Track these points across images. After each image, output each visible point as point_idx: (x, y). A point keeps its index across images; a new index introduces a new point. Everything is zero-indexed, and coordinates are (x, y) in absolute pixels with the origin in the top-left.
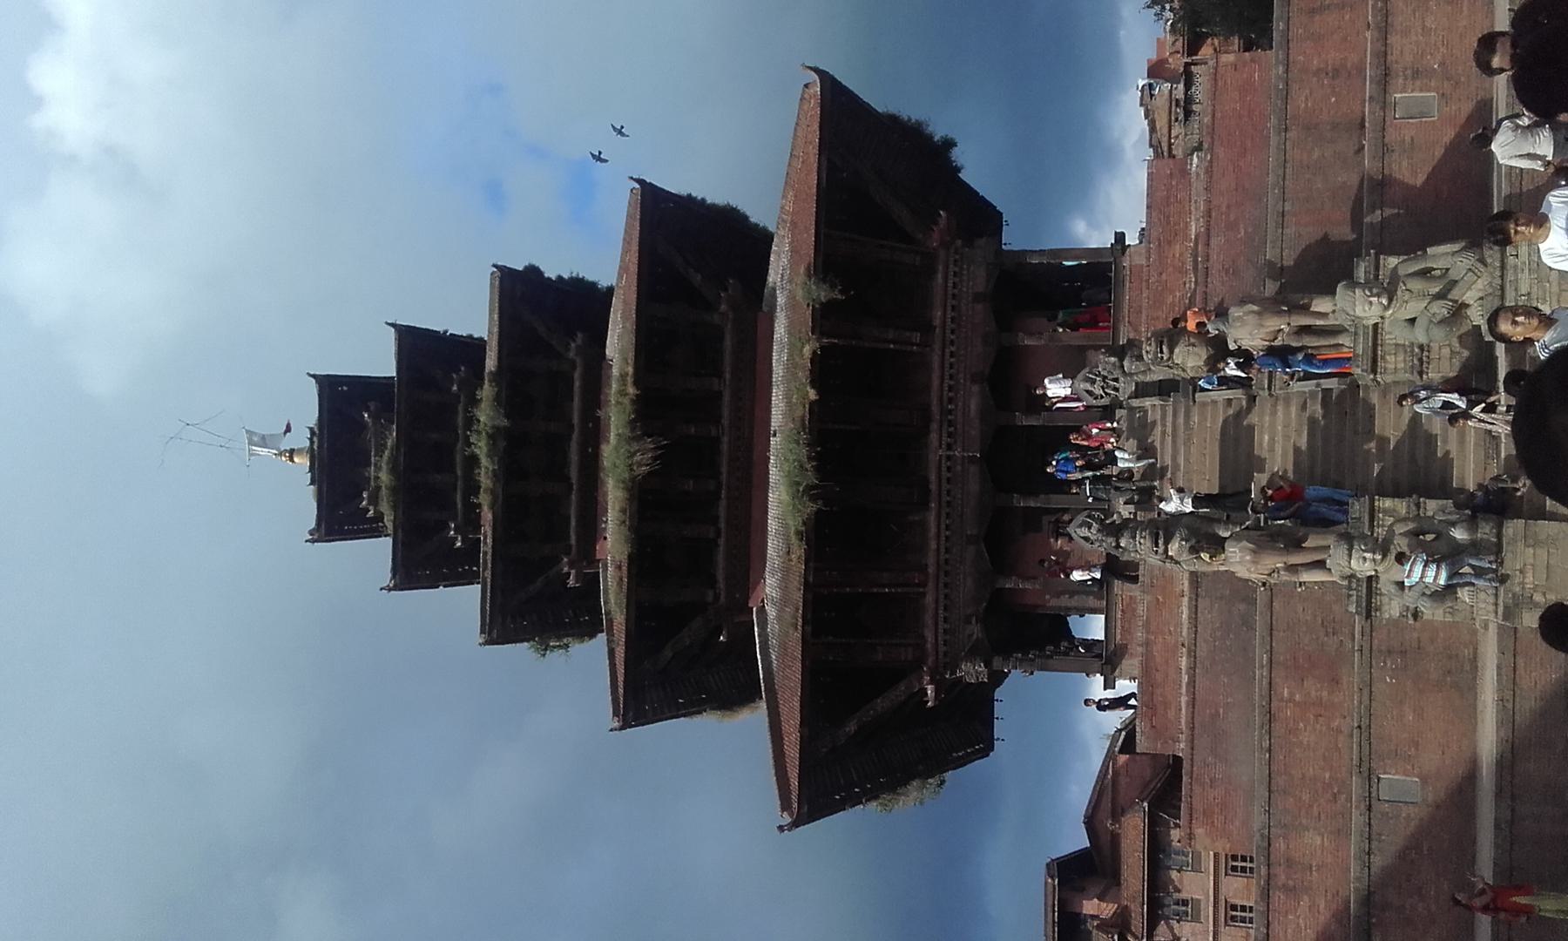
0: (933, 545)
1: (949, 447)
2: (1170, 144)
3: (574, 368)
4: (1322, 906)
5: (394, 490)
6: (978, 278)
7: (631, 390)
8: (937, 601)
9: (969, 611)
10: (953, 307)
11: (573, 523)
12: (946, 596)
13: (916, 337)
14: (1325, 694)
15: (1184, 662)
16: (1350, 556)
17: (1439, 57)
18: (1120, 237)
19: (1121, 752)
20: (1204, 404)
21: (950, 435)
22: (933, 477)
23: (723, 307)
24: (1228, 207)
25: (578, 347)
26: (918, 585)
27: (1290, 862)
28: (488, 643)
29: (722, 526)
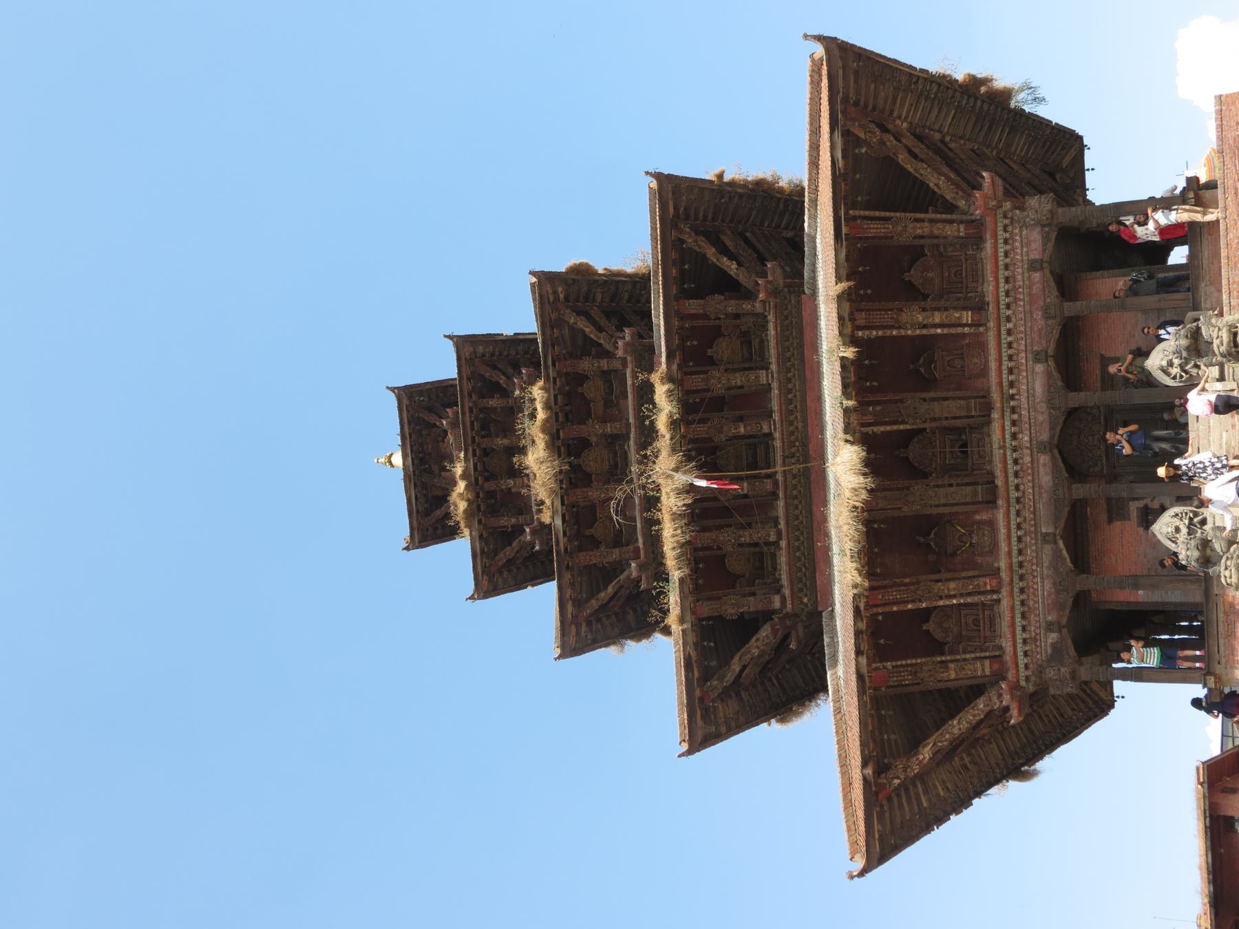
3: (625, 365)
8: (1013, 609)
10: (1007, 280)
12: (1023, 603)
13: (967, 317)
21: (1014, 423)
22: (998, 472)
23: (762, 296)
25: (626, 344)
26: (993, 592)
29: (782, 525)
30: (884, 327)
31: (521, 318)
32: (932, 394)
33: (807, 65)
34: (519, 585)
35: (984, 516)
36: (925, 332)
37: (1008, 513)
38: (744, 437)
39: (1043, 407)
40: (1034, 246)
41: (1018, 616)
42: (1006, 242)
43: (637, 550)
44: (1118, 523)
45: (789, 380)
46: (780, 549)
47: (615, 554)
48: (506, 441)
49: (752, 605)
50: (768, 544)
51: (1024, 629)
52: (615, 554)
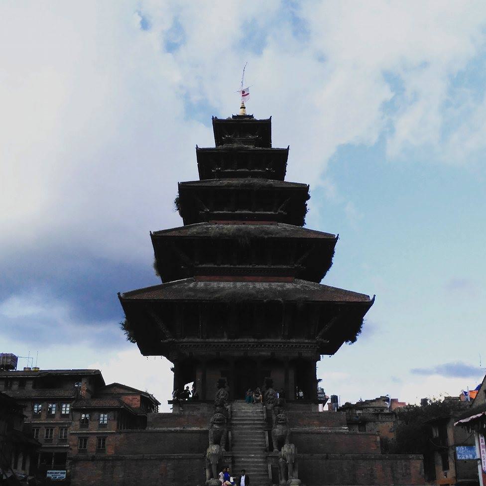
0: (215, 341)
2: (367, 408)
4: (99, 478)
5: (231, 149)
6: (307, 354)
7: (266, 237)
8: (197, 342)
9: (193, 353)
11: (221, 212)
14: (169, 477)
15: (178, 428)
19: (141, 396)
20: (264, 434)
21: (253, 345)
22: (239, 340)
28: (179, 184)
34: (198, 161)
35: (225, 334)
37: (225, 342)
46: (214, 265)
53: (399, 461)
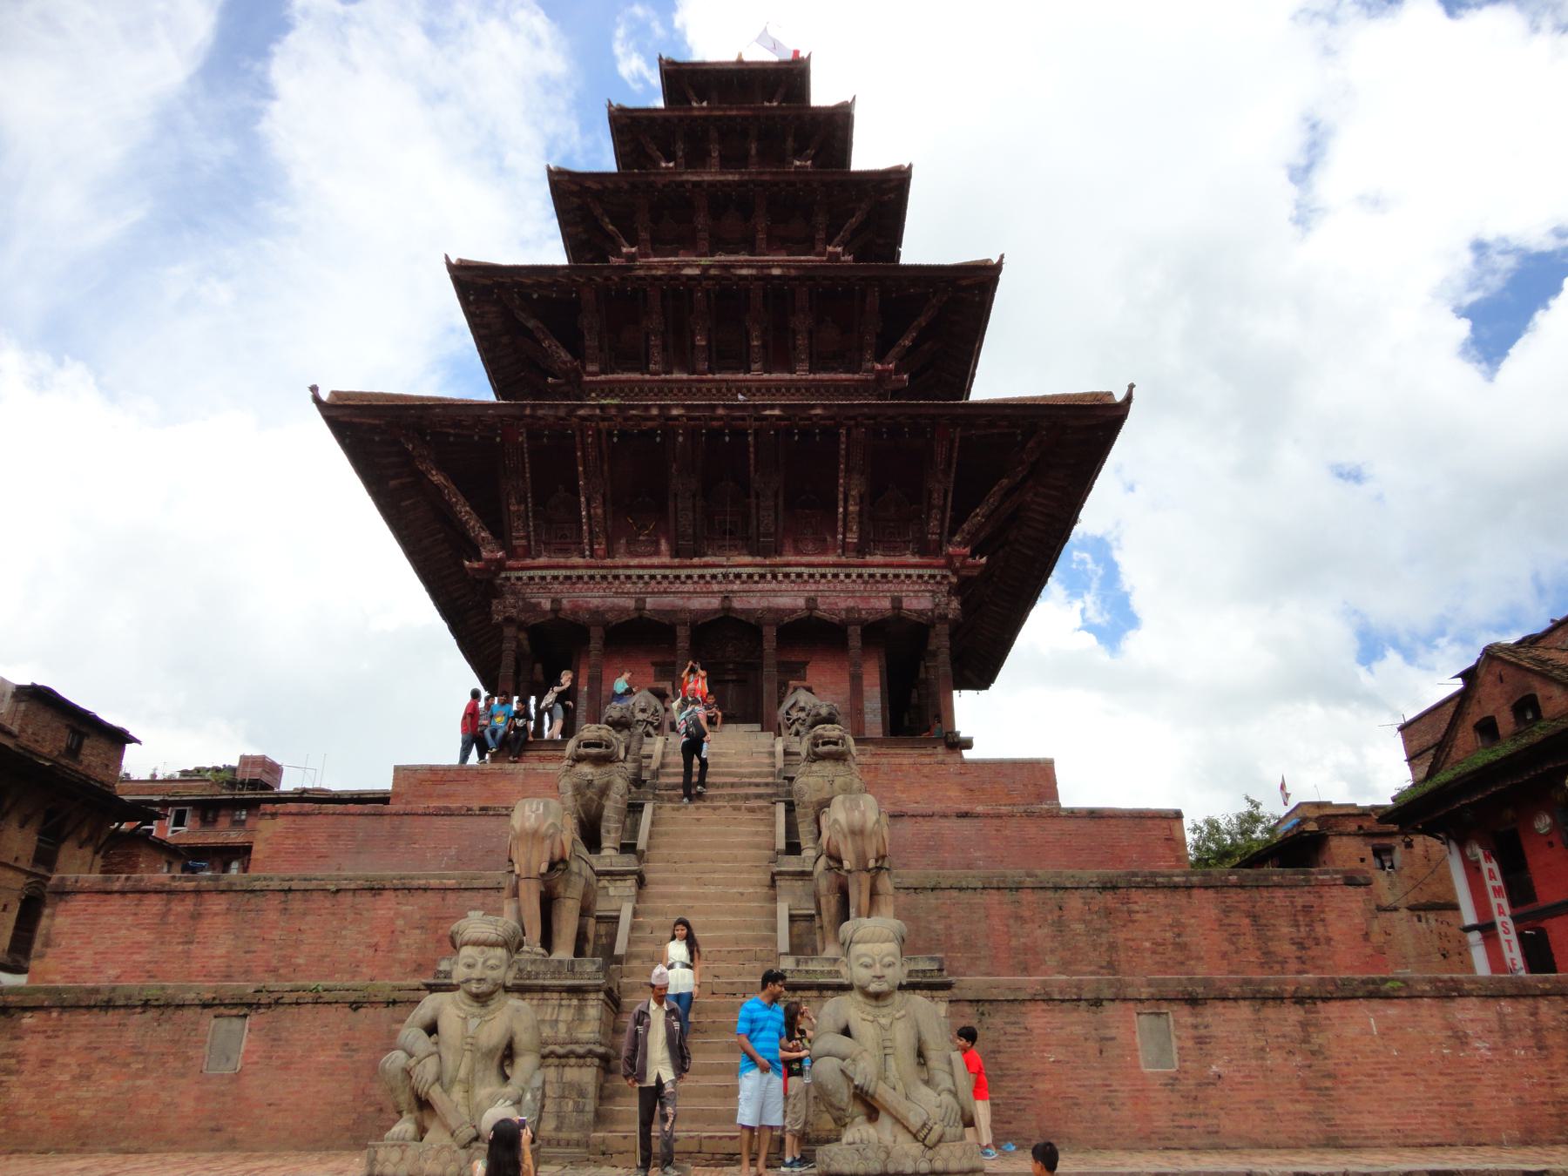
1: (738, 576)
4: (137, 957)
9: (565, 602)
10: (884, 576)
12: (580, 578)
13: (853, 538)
14: (403, 956)
16: (476, 943)
17: (1223, 1071)
18: (968, 744)
21: (750, 576)
23: (879, 366)
24: (1007, 837)
25: (837, 254)
26: (592, 550)
27: (196, 916)
28: (550, 171)
30: (847, 455)
31: (866, 156)
32: (781, 503)
33: (1105, 390)
35: (664, 546)
36: (841, 496)
38: (748, 341)
39: (764, 603)
40: (915, 602)
41: (568, 573)
42: (920, 577)
43: (647, 256)
44: (652, 670)
45: (798, 390)
47: (644, 235)
48: (753, 152)
49: (591, 342)
50: (648, 364)
51: (555, 578)
52: (644, 235)
53: (1280, 893)
